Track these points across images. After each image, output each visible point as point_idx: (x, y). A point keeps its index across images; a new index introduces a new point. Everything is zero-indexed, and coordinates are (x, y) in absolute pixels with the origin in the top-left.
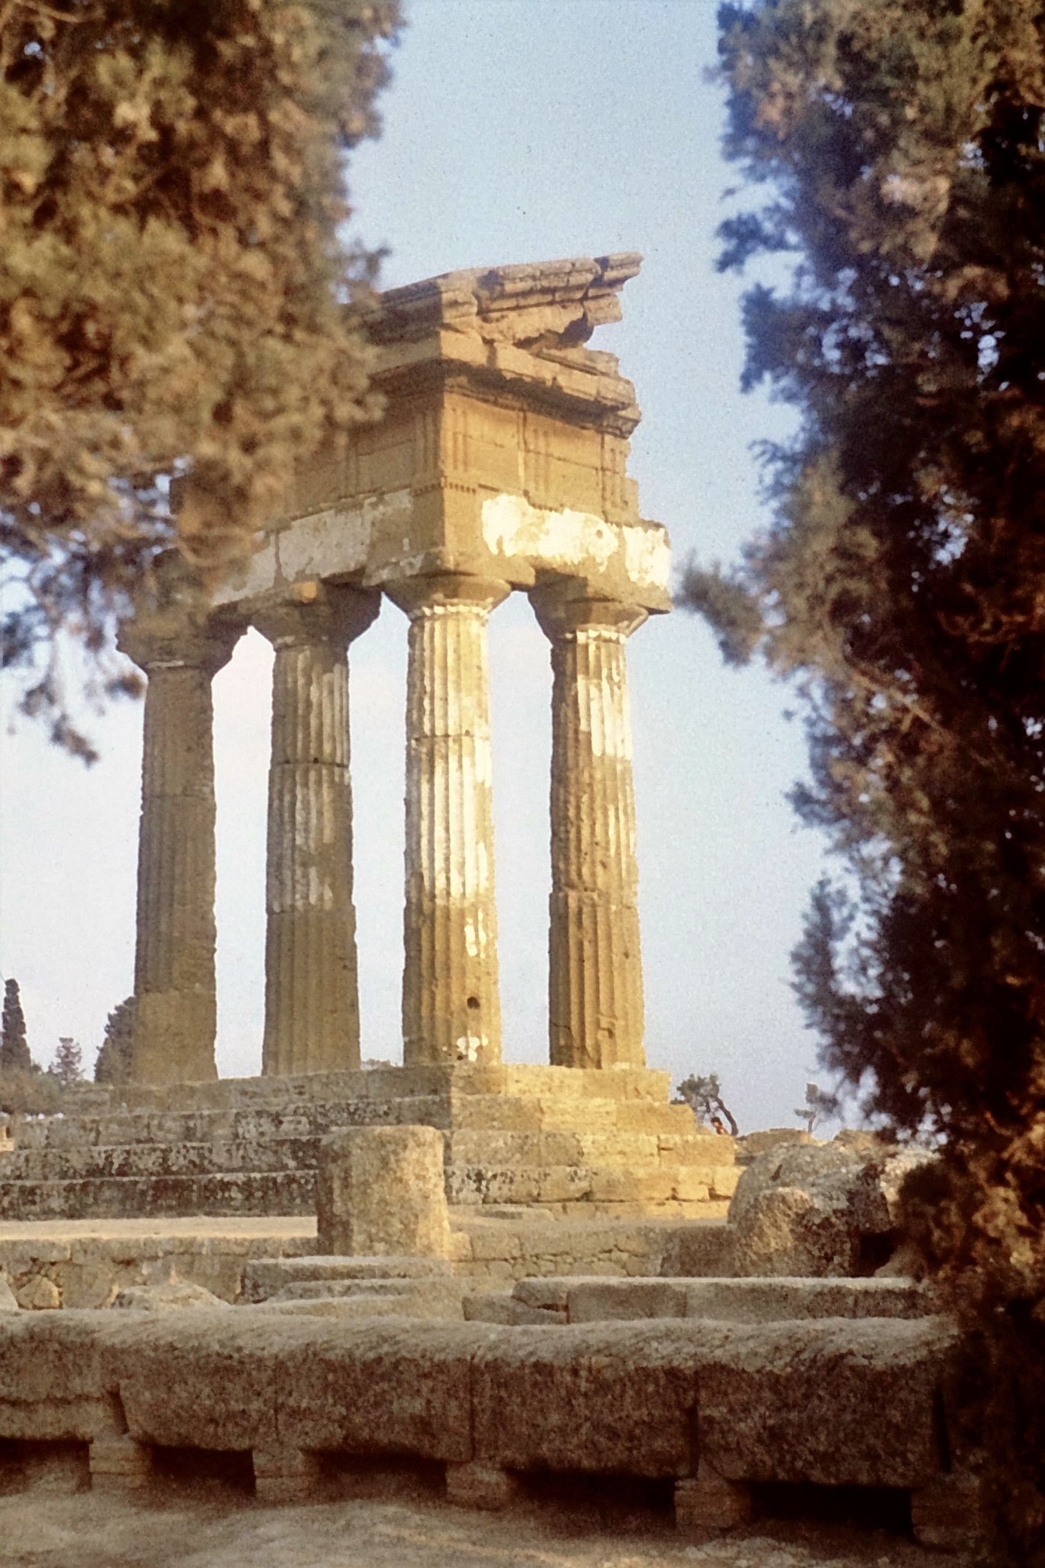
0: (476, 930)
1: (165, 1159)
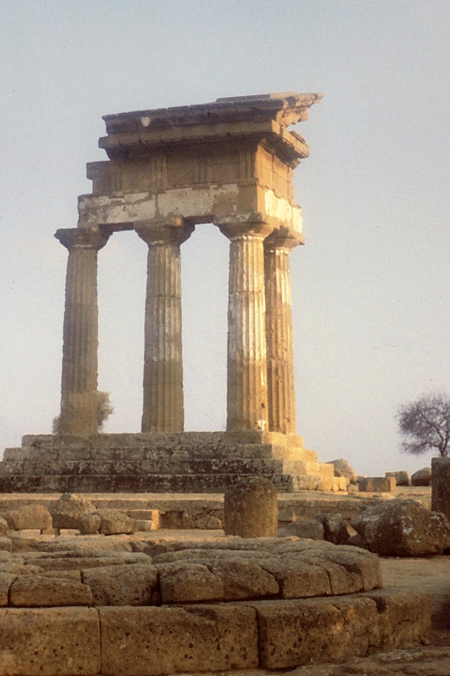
1: (113, 467)
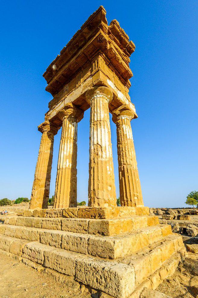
0: (110, 167)
